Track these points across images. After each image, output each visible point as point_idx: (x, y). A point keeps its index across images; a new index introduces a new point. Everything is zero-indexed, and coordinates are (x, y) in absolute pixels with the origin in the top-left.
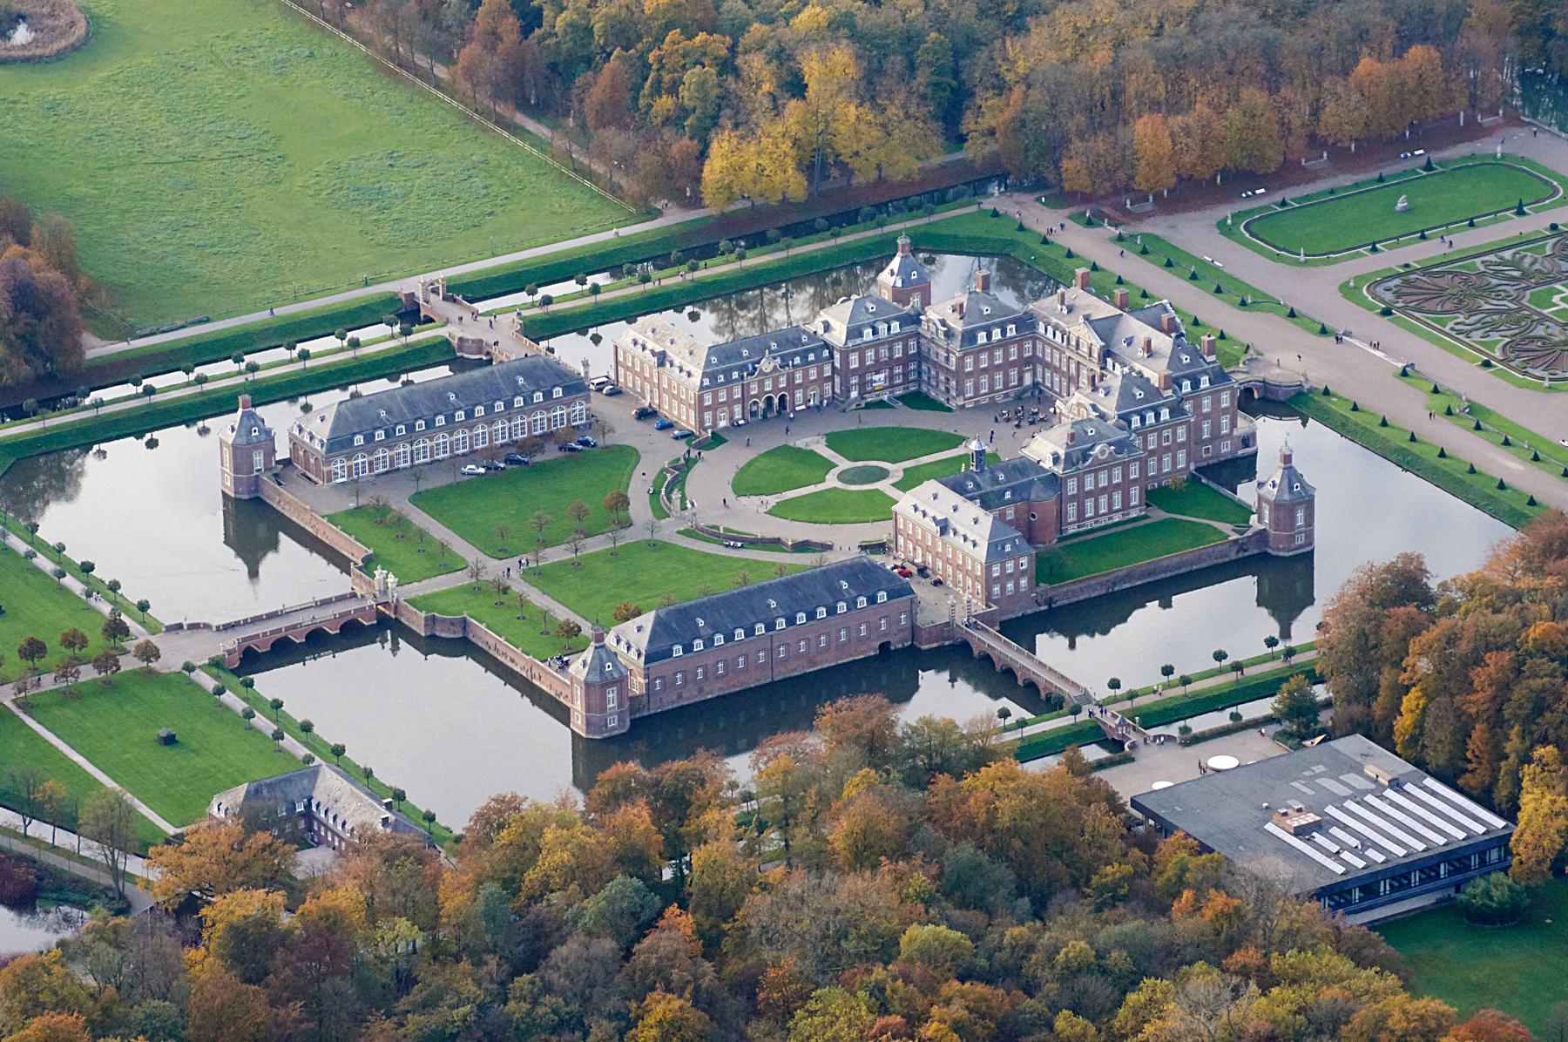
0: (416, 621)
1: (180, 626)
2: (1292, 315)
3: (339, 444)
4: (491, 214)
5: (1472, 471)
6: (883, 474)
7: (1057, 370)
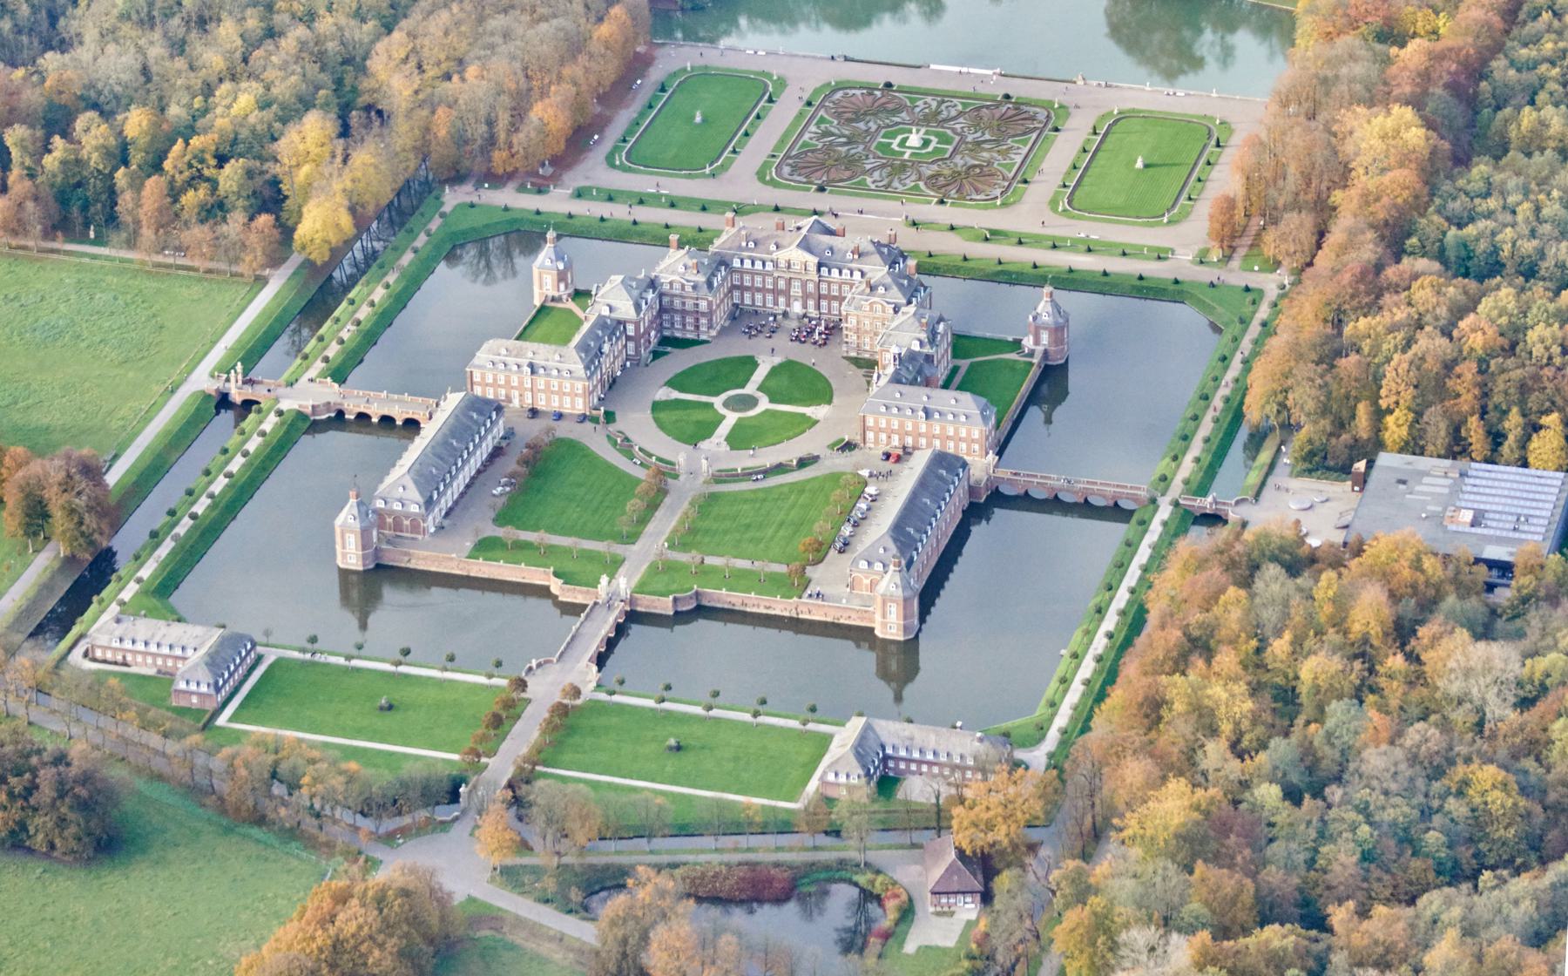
0: (665, 606)
1: (530, 669)
2: (777, 209)
3: (429, 503)
4: (154, 316)
5: (1071, 271)
6: (751, 402)
7: (762, 290)
